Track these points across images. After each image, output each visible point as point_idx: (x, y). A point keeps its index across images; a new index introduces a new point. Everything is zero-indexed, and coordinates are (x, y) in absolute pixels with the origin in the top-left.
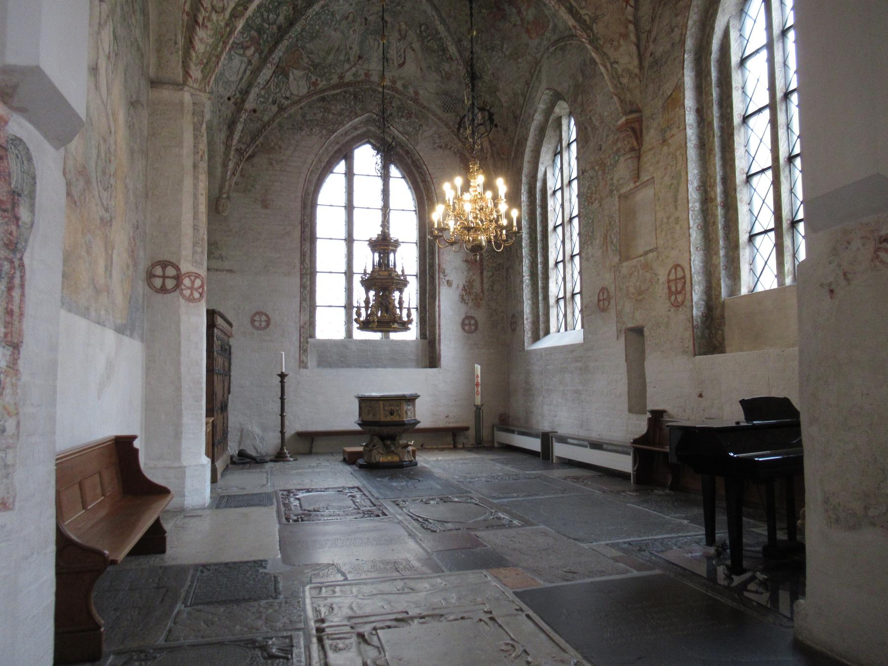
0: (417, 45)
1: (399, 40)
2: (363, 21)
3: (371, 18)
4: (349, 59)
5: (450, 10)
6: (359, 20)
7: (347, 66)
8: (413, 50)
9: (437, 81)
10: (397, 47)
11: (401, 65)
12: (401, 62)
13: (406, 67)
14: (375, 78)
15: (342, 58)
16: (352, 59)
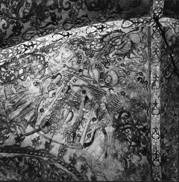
0: (110, 129)
1: (94, 119)
2: (66, 88)
3: (76, 89)
4: (35, 122)
5: (165, 106)
6: (63, 85)
7: (29, 129)
8: (105, 133)
9: (119, 171)
10: (89, 126)
11: (87, 145)
12: (88, 141)
13: (92, 147)
14: (55, 151)
15: (28, 118)
16: (38, 123)
